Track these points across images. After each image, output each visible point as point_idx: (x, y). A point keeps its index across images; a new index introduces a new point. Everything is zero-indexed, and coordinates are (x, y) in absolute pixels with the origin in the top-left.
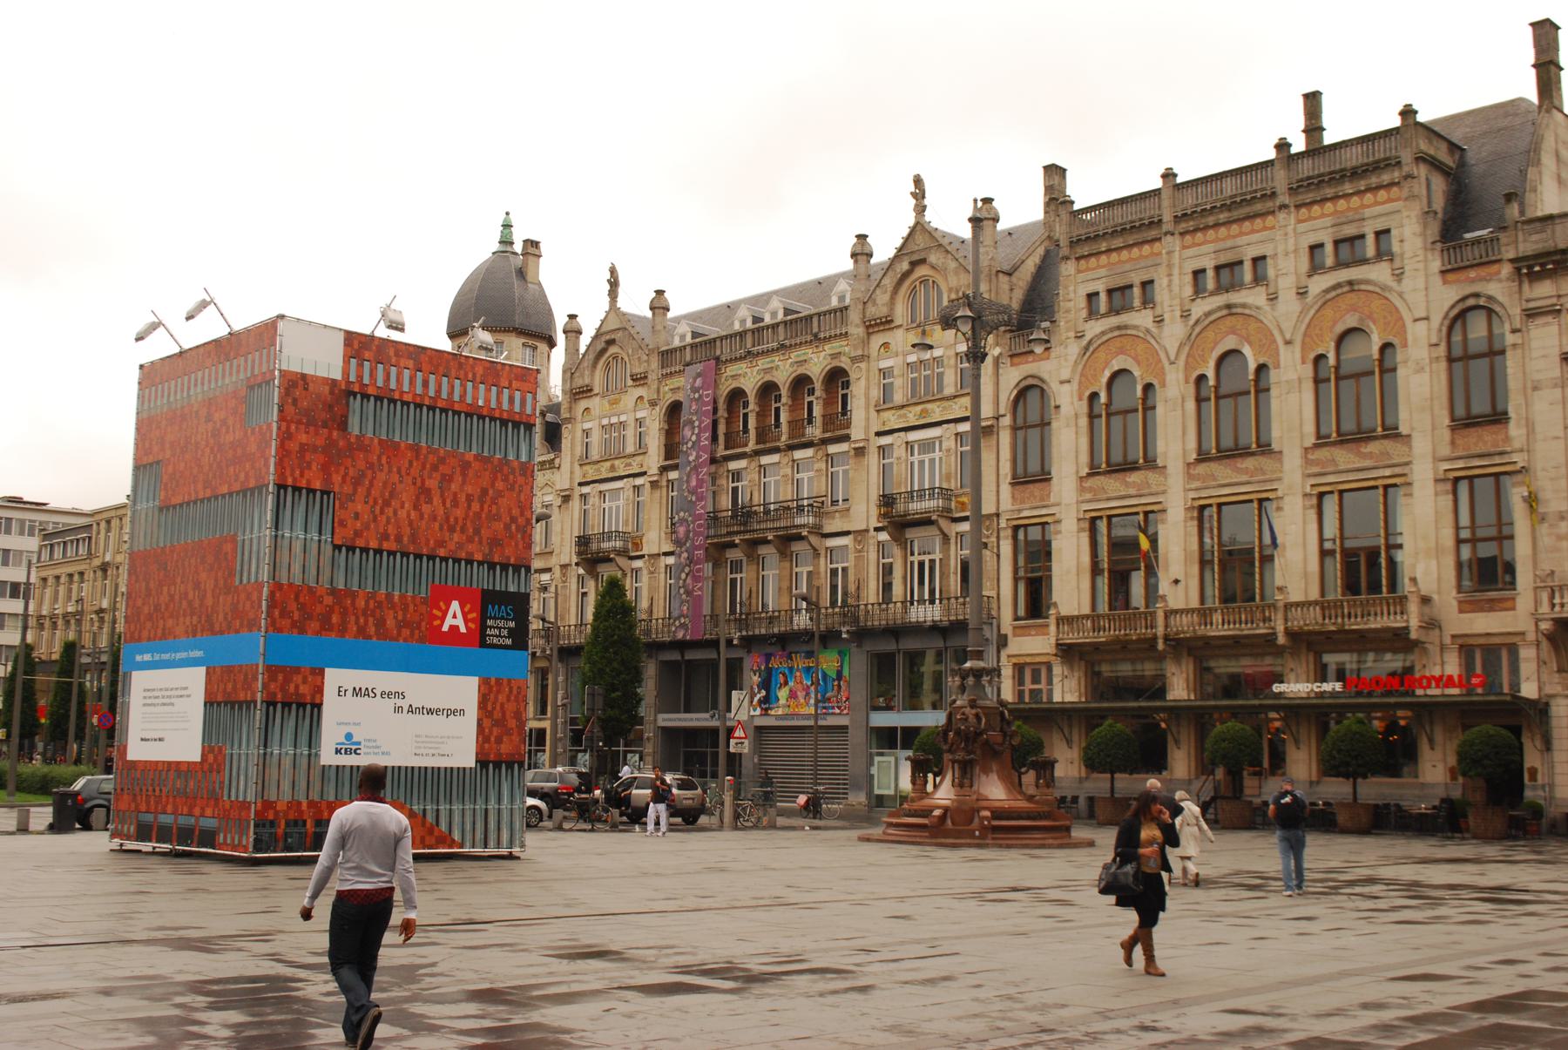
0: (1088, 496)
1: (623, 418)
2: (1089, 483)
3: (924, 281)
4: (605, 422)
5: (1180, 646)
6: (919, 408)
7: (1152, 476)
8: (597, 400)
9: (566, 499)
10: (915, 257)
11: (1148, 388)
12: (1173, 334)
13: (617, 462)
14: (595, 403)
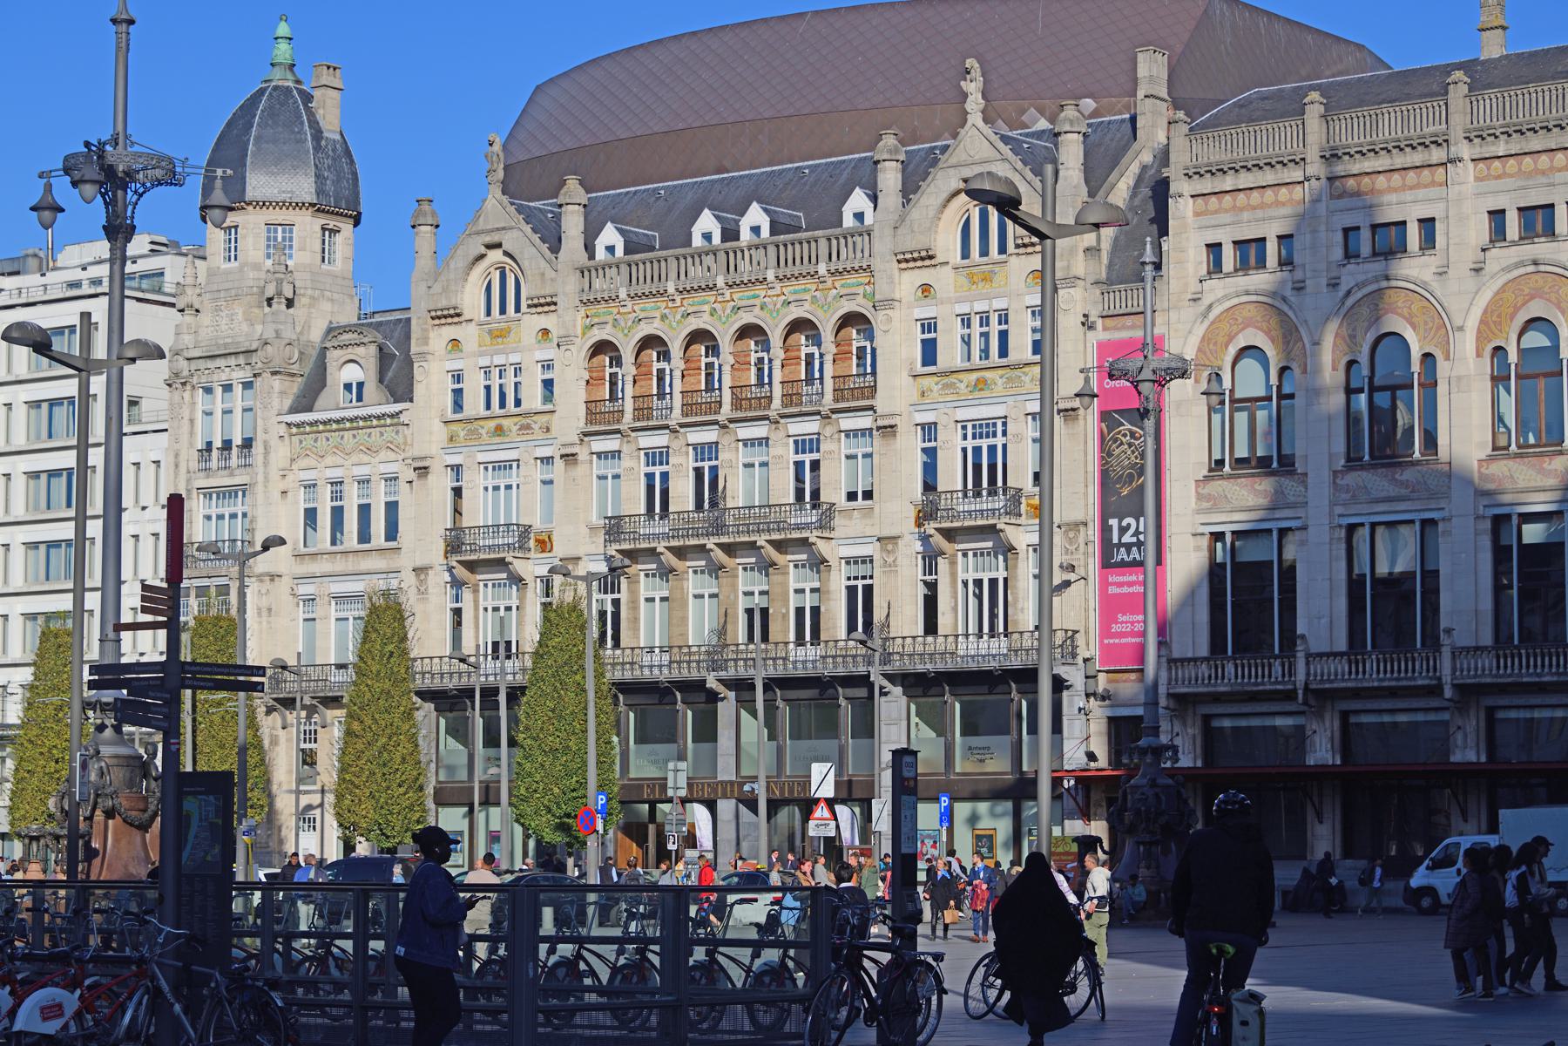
0: (1205, 505)
5: (1320, 697)
6: (974, 376)
9: (423, 471)
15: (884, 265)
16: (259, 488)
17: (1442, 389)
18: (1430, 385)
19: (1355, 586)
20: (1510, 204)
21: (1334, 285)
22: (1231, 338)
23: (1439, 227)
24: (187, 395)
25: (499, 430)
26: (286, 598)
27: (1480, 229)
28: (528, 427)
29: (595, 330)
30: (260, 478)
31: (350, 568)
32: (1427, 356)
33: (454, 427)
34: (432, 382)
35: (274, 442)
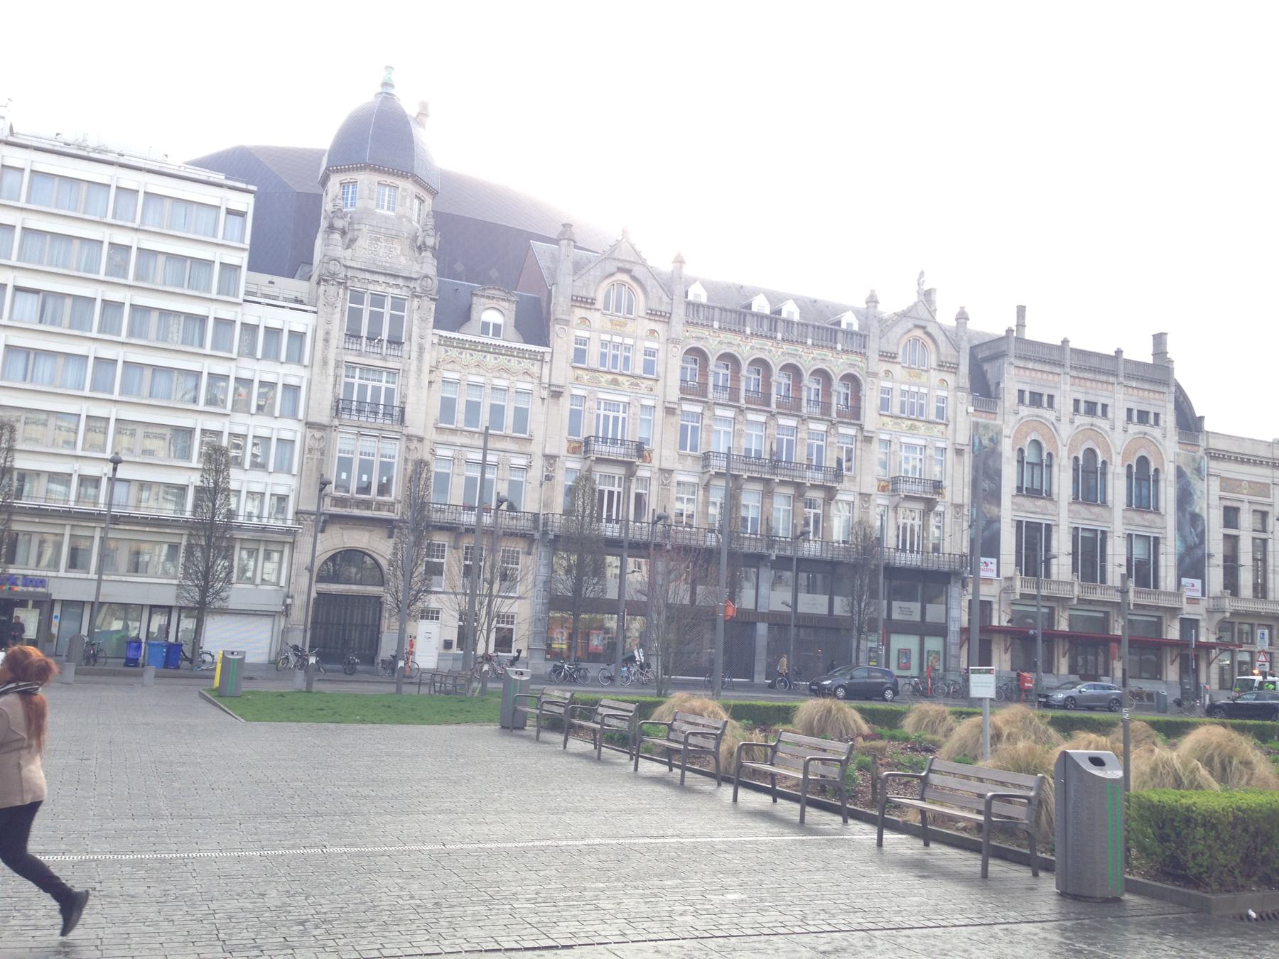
1: (629, 341)
3: (917, 340)
4: (606, 337)
6: (910, 422)
7: (1049, 505)
8: (598, 314)
9: (557, 395)
10: (918, 323)
13: (620, 378)
14: (595, 317)
15: (873, 355)
16: (412, 376)
17: (1109, 477)
18: (1104, 474)
19: (1129, 561)
20: (1135, 407)
22: (1028, 434)
23: (1110, 410)
24: (341, 291)
25: (615, 382)
27: (1123, 415)
28: (637, 385)
29: (724, 346)
32: (1104, 463)
33: (580, 372)
34: (563, 340)
35: (428, 346)
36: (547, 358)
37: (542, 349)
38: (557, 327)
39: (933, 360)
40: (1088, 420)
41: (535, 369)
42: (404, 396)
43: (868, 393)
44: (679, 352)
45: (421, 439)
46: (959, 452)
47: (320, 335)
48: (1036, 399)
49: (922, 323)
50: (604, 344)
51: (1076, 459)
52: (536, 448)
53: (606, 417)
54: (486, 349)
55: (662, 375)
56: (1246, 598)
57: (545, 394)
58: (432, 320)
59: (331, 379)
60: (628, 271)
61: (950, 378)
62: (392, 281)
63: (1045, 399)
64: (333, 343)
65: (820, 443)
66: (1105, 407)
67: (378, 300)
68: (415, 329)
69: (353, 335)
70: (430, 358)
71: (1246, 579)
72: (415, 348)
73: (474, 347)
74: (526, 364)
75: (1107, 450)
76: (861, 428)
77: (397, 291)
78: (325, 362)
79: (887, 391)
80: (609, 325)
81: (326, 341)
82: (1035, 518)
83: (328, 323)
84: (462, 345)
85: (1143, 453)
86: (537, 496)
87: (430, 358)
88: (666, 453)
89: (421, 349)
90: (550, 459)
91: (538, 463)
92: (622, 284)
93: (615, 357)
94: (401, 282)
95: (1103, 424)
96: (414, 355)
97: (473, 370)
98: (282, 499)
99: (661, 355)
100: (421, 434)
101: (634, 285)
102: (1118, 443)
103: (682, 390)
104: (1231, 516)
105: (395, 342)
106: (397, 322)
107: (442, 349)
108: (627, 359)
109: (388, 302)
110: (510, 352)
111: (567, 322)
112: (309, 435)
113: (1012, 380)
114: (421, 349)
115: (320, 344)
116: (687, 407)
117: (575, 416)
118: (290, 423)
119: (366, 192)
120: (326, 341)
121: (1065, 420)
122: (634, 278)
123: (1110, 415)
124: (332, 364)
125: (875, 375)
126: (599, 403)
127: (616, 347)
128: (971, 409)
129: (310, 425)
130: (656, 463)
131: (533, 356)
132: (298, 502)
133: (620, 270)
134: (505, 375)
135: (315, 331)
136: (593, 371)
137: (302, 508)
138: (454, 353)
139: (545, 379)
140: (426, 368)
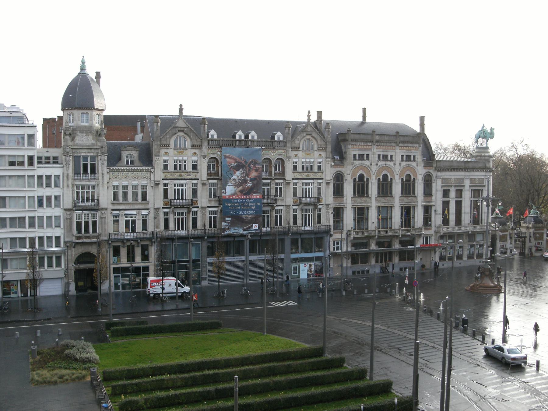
1: (185, 159)
2: (353, 199)
3: (308, 139)
4: (176, 158)
7: (367, 199)
8: (172, 150)
9: (157, 185)
11: (368, 179)
12: (374, 168)
13: (183, 174)
14: (171, 151)
16: (100, 186)
21: (377, 165)
23: (393, 156)
26: (109, 215)
27: (399, 158)
30: (101, 183)
31: (132, 207)
34: (159, 163)
36: (152, 170)
37: (150, 168)
38: (155, 158)
39: (315, 147)
40: (384, 163)
41: (148, 175)
42: (98, 194)
43: (287, 164)
44: (207, 160)
45: (106, 209)
46: (328, 184)
47: (65, 175)
48: (361, 157)
49: (310, 133)
50: (175, 161)
51: (379, 179)
52: (150, 206)
53: (178, 190)
54: (128, 171)
55: (199, 170)
56: (452, 227)
57: (153, 185)
58: (106, 163)
59: (71, 192)
60: (183, 131)
61: (323, 154)
62: (89, 151)
63: (365, 156)
64: (70, 178)
65: (268, 187)
66: (391, 156)
67: (85, 159)
68: (100, 168)
69: (77, 173)
70: (107, 177)
71: (452, 218)
72: (100, 175)
73: (123, 170)
74: (144, 174)
75: (392, 173)
76: (284, 179)
77: (92, 154)
78: (68, 186)
79: (296, 162)
80: (177, 153)
81: (67, 177)
82: (360, 205)
83: (68, 171)
84: (119, 170)
85: (408, 172)
86: (153, 224)
87: (107, 177)
88: (203, 200)
89: (103, 174)
90: (157, 209)
91: (152, 211)
92: (180, 136)
93: (180, 165)
94: (93, 151)
95: (390, 164)
96: (100, 178)
97: (124, 180)
98: (58, 238)
99: (198, 162)
100: (106, 207)
101: (186, 136)
102: (397, 170)
103: (209, 174)
104: (446, 193)
105: (93, 172)
106: (93, 166)
107: (111, 173)
108: (185, 166)
109: (89, 159)
110: (138, 170)
111: (159, 155)
112: (65, 214)
113: (352, 150)
114: (103, 174)
115: (65, 178)
116: (211, 181)
117: (166, 192)
118: (58, 210)
119: (77, 119)
120: (67, 177)
121: (374, 164)
122: (185, 133)
123: (394, 159)
124: (70, 186)
125: (290, 157)
126: (175, 185)
127: (180, 161)
128: (333, 164)
129: (66, 210)
130: (199, 205)
131: (147, 171)
132: (64, 239)
133: (179, 131)
134: (136, 180)
135: (63, 174)
136: (171, 172)
137: (66, 240)
138: (116, 174)
139: (152, 179)
140: (105, 182)
